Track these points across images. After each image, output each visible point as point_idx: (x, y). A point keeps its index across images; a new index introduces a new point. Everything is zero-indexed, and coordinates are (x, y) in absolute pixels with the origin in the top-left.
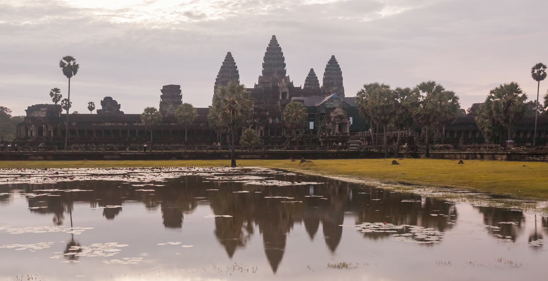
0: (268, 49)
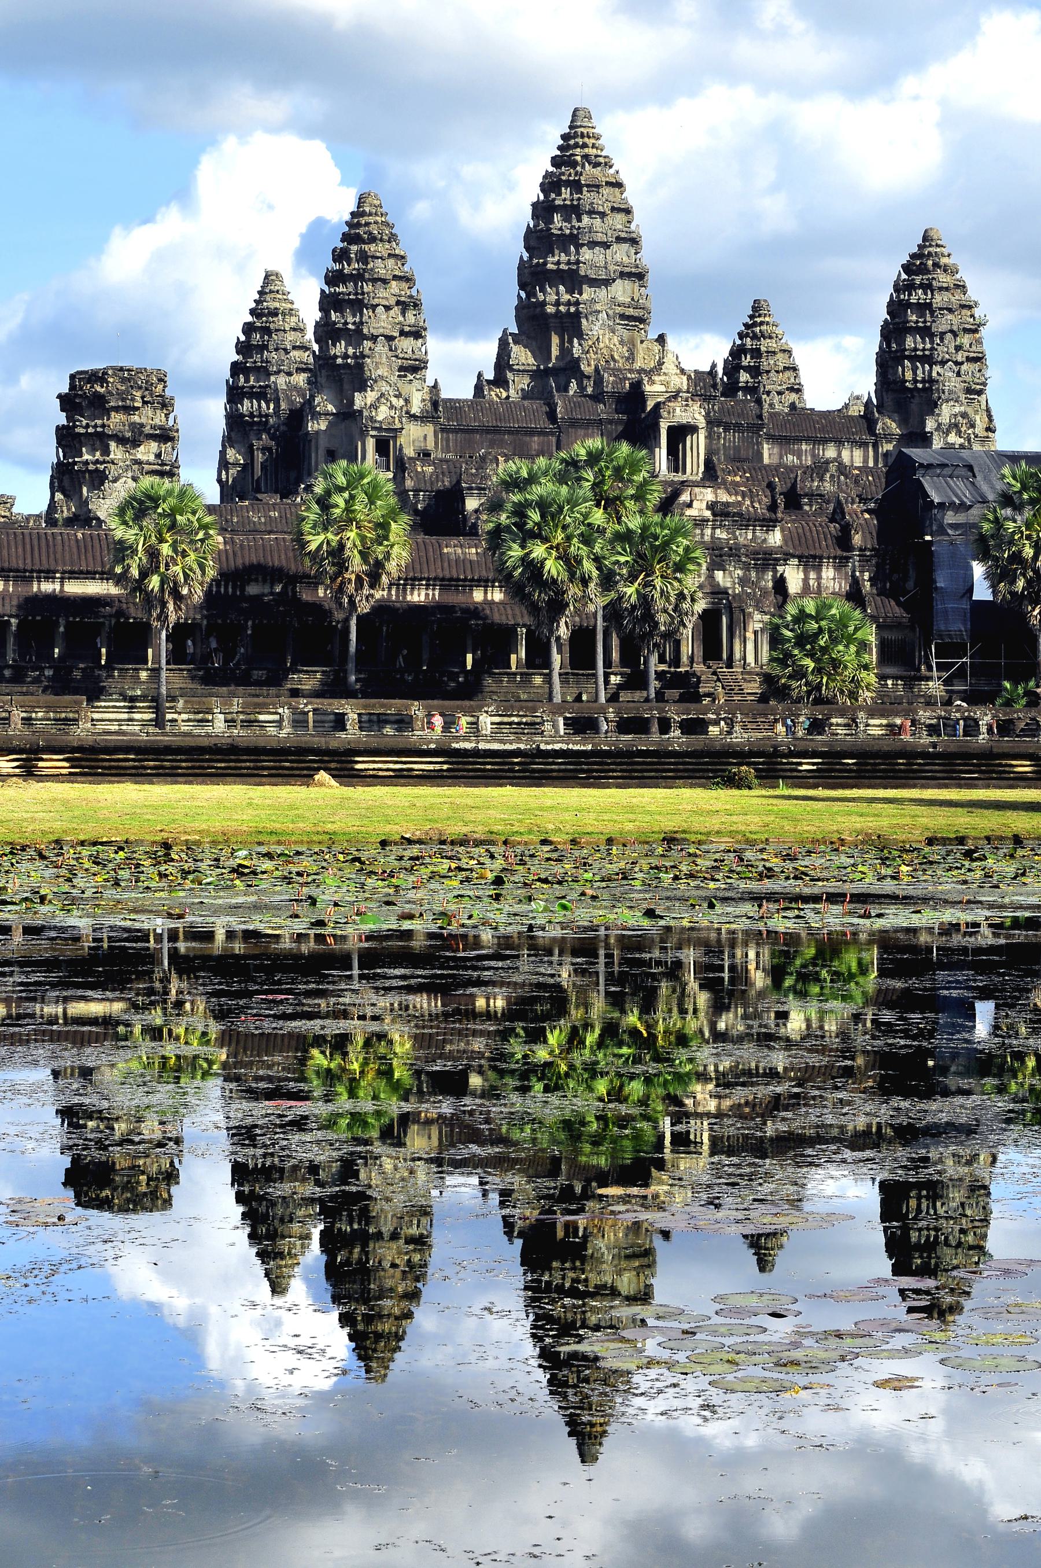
0: (550, 184)
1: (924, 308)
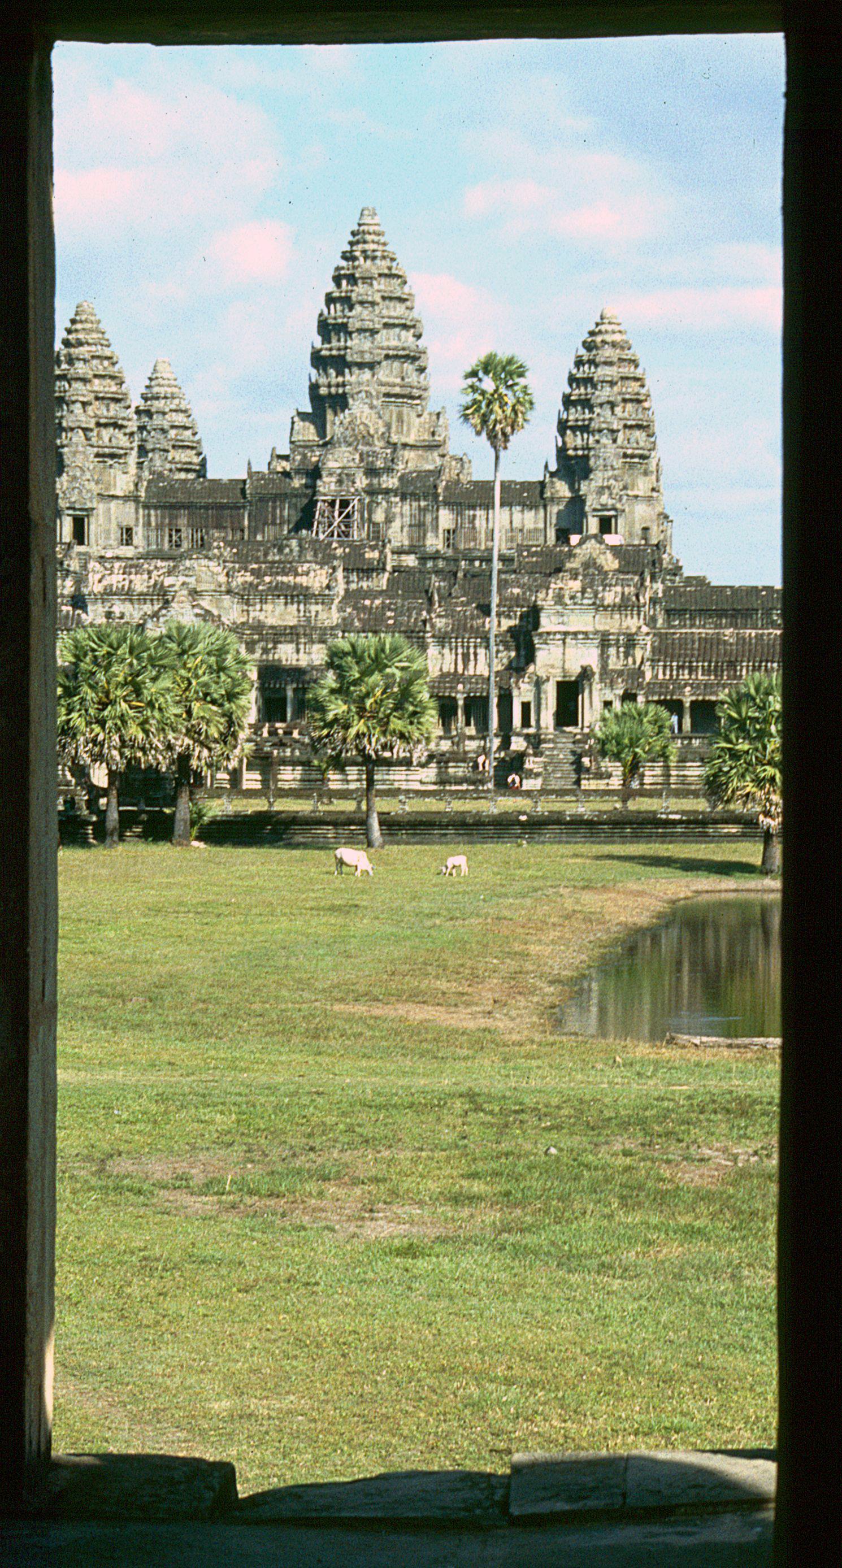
1: (588, 381)
